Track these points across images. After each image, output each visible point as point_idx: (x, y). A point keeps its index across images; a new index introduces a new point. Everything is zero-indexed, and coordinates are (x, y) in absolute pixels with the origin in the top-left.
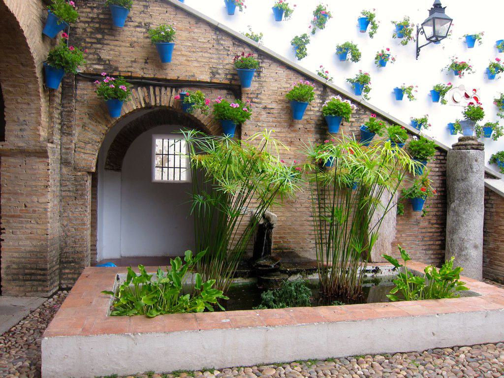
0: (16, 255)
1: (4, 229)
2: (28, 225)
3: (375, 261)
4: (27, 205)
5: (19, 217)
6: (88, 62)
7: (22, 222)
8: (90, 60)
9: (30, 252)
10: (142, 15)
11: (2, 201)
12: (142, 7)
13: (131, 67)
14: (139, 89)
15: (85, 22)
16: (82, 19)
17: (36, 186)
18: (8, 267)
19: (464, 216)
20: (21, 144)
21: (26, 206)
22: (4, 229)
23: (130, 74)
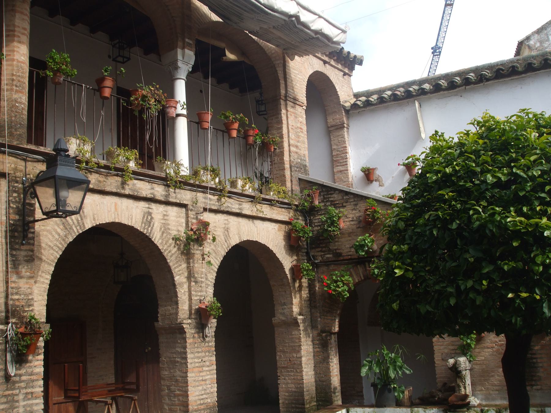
0: (287, 394)
1: (279, 376)
2: (292, 374)
4: (291, 359)
5: (287, 368)
6: (322, 253)
7: (288, 372)
8: (324, 252)
9: (295, 392)
10: (354, 212)
11: (277, 358)
12: (353, 206)
13: (350, 251)
14: (358, 266)
15: (317, 226)
16: (316, 224)
17: (294, 346)
20: (283, 318)
21: (290, 360)
22: (279, 376)
23: (350, 257)
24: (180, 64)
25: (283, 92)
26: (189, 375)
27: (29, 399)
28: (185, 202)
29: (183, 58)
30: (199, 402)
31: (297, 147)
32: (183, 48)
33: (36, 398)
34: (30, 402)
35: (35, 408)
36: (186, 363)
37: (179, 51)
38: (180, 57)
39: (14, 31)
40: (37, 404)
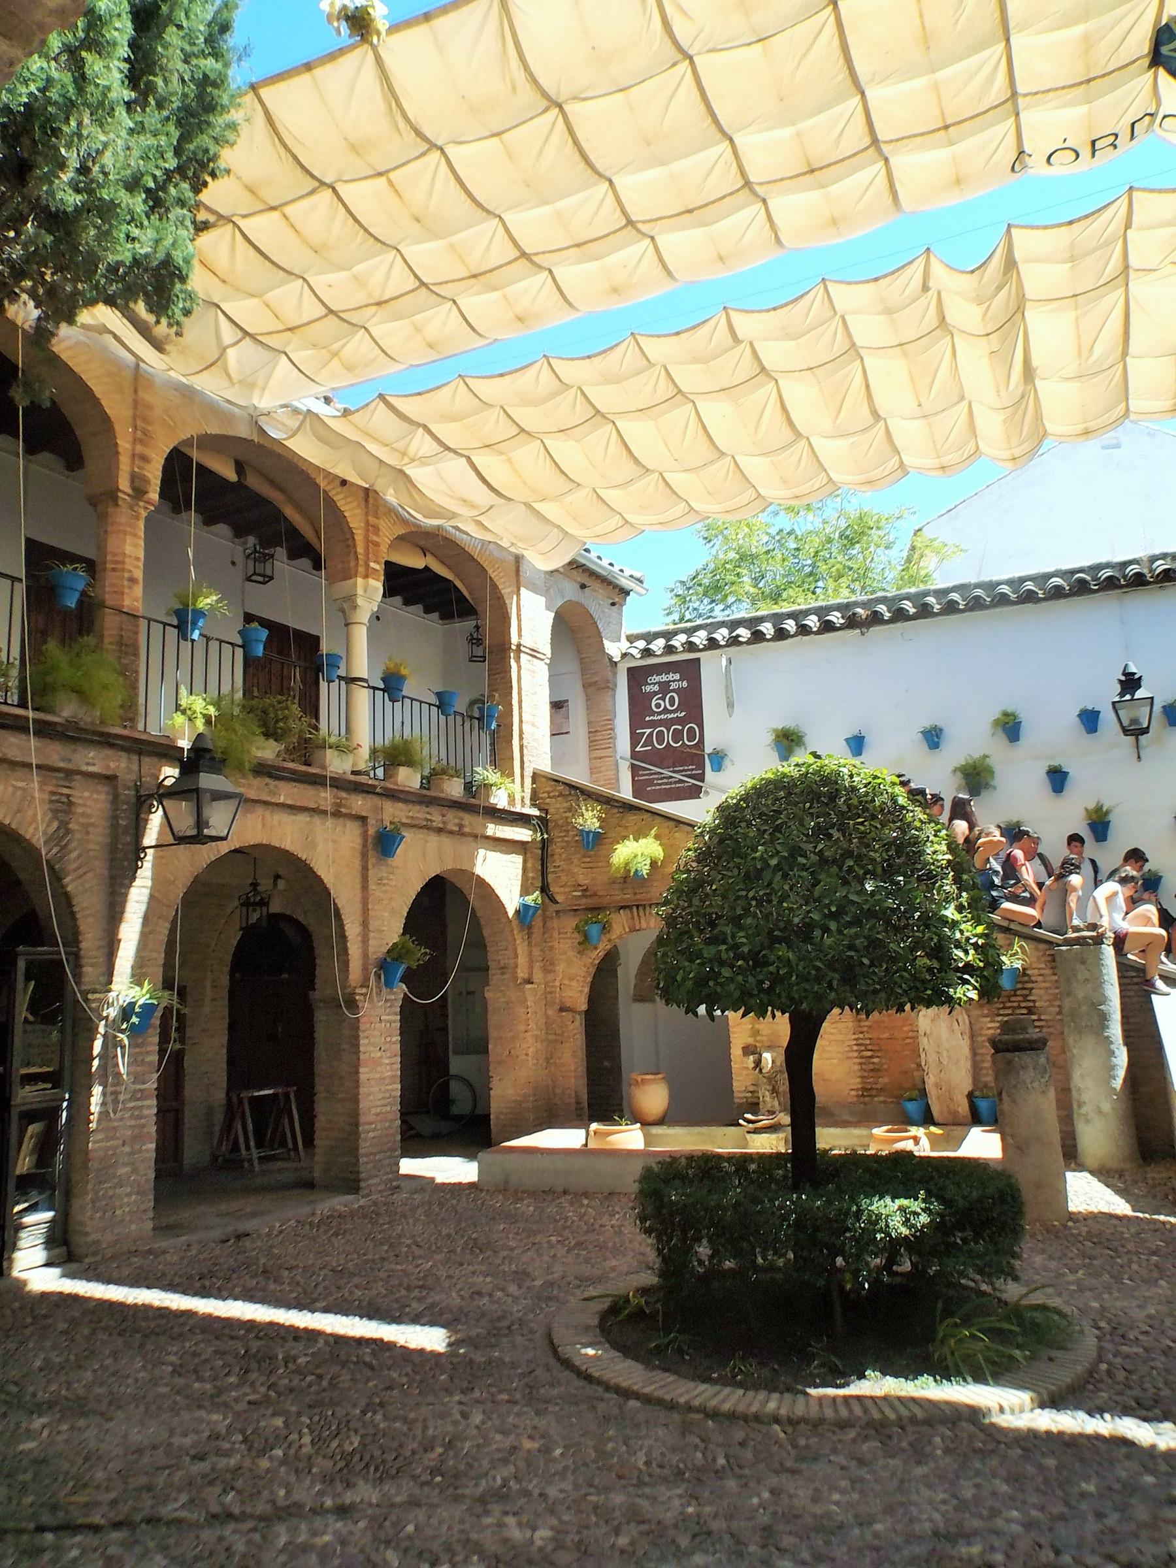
3: (940, 1121)
18: (497, 1118)
19: (1075, 1051)
24: (360, 601)
25: (514, 640)
26: (362, 1070)
27: (138, 1100)
28: (364, 814)
29: (365, 591)
30: (374, 1111)
31: (533, 725)
32: (366, 576)
33: (147, 1098)
34: (139, 1103)
35: (146, 1112)
36: (358, 1052)
37: (360, 581)
38: (360, 591)
39: (123, 563)
40: (149, 1107)
